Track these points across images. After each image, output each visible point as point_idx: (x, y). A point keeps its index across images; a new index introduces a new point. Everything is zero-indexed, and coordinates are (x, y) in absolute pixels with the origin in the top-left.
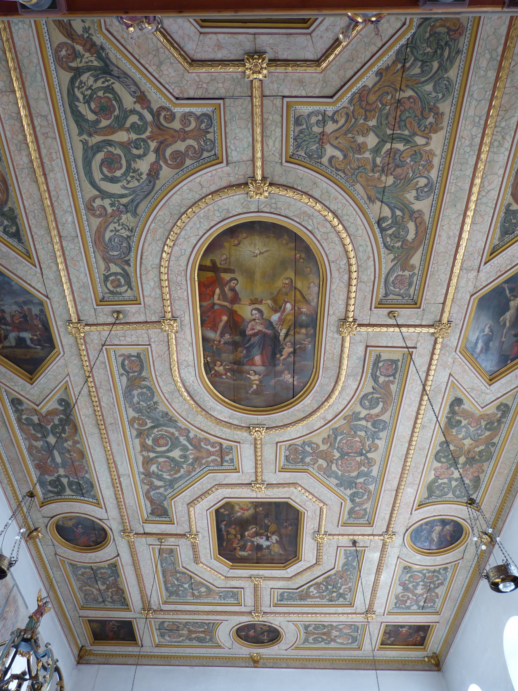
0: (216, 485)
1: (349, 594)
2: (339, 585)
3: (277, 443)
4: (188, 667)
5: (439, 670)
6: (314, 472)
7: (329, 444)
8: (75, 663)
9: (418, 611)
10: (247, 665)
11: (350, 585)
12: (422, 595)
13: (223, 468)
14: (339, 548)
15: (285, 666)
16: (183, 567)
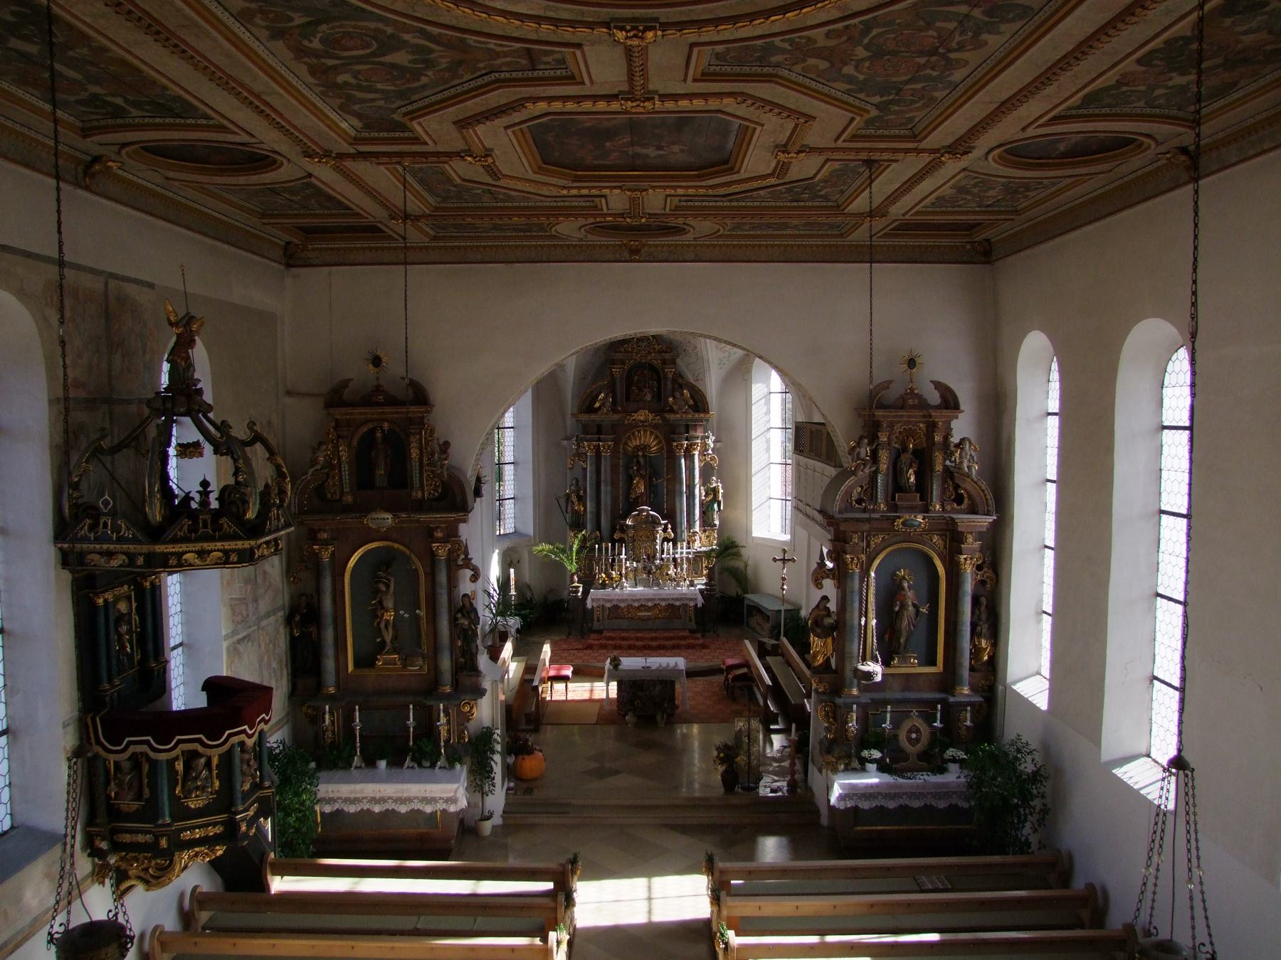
0: (522, 99)
1: (838, 196)
2: (818, 188)
3: (692, 45)
4: (502, 265)
5: (988, 263)
6: (793, 76)
7: (845, 38)
8: (282, 267)
9: (977, 209)
10: (617, 256)
11: (842, 187)
12: (993, 197)
13: (536, 74)
14: (829, 163)
15: (692, 258)
16: (464, 180)
